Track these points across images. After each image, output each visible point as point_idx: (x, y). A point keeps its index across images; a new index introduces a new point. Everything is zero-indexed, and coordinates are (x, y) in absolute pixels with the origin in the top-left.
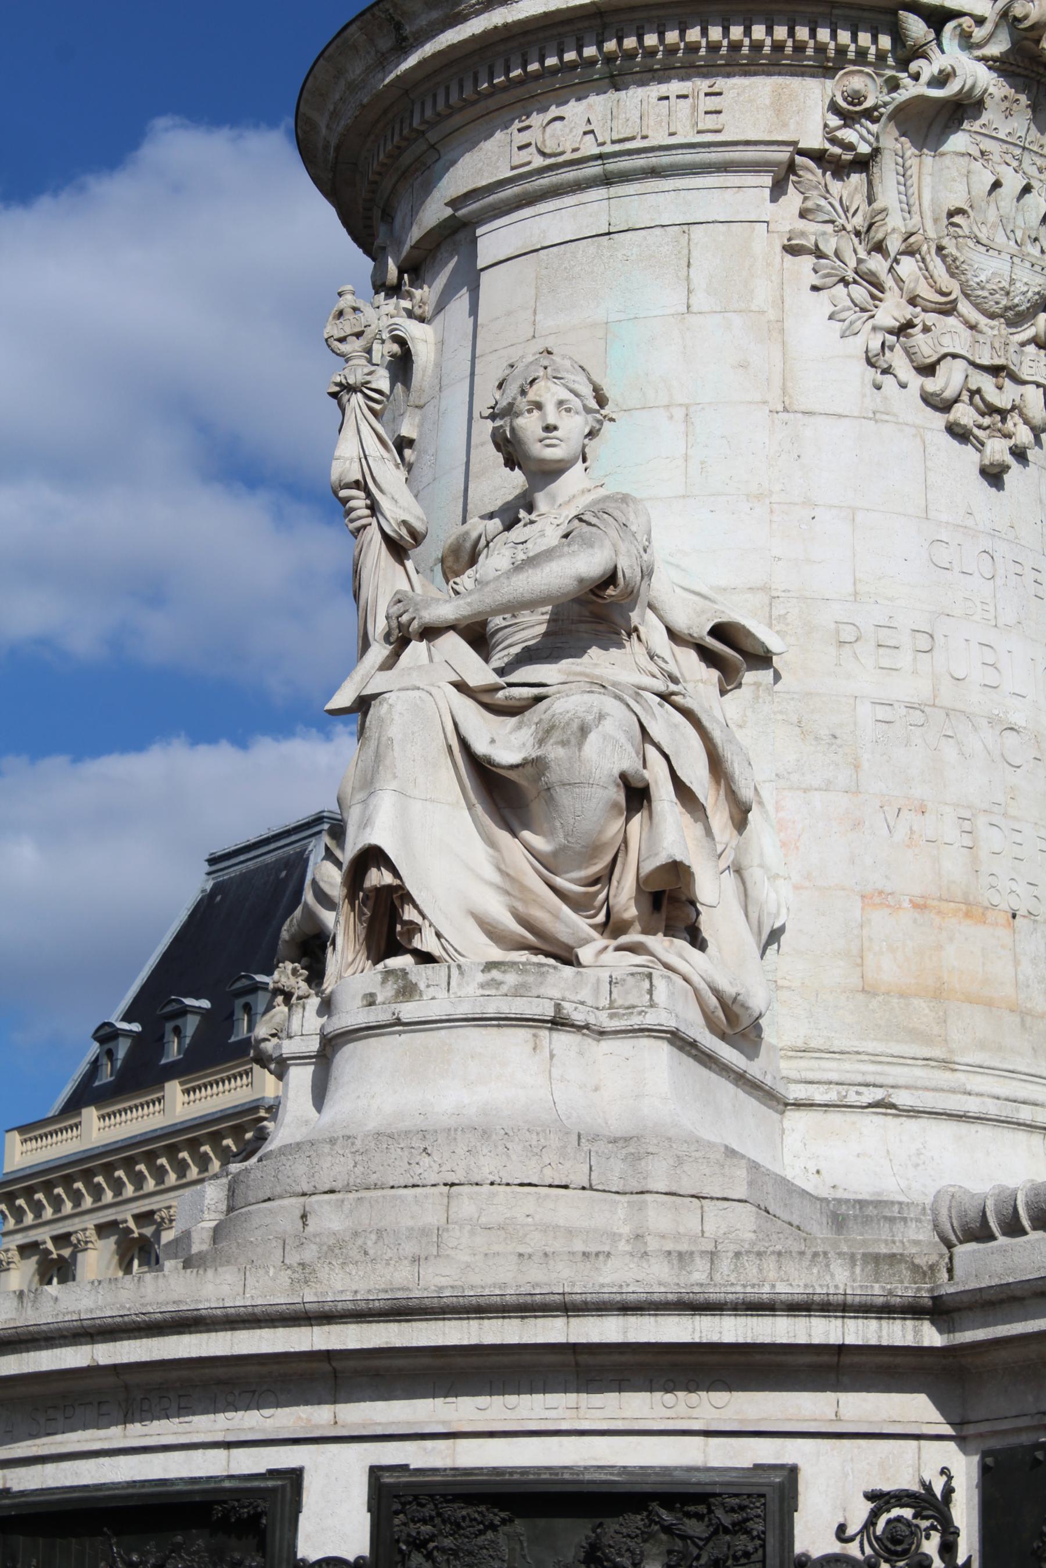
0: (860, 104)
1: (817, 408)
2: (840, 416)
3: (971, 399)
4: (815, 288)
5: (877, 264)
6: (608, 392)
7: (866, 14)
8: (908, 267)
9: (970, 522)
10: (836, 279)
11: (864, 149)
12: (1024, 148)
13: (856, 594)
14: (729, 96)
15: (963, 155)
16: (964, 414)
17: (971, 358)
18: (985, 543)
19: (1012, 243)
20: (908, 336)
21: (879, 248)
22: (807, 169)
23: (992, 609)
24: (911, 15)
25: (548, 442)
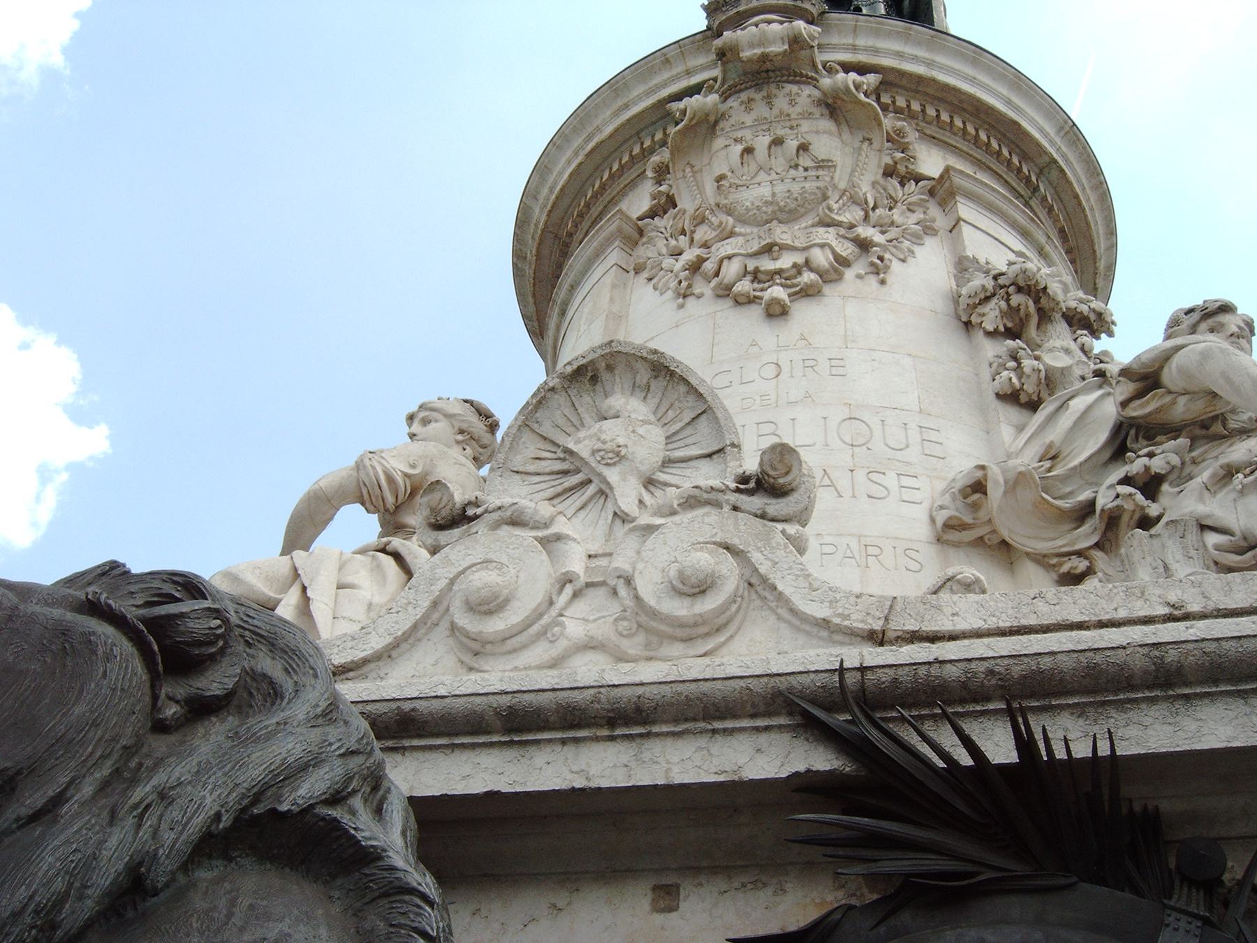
16: (745, 286)
21: (683, 233)
22: (647, 225)
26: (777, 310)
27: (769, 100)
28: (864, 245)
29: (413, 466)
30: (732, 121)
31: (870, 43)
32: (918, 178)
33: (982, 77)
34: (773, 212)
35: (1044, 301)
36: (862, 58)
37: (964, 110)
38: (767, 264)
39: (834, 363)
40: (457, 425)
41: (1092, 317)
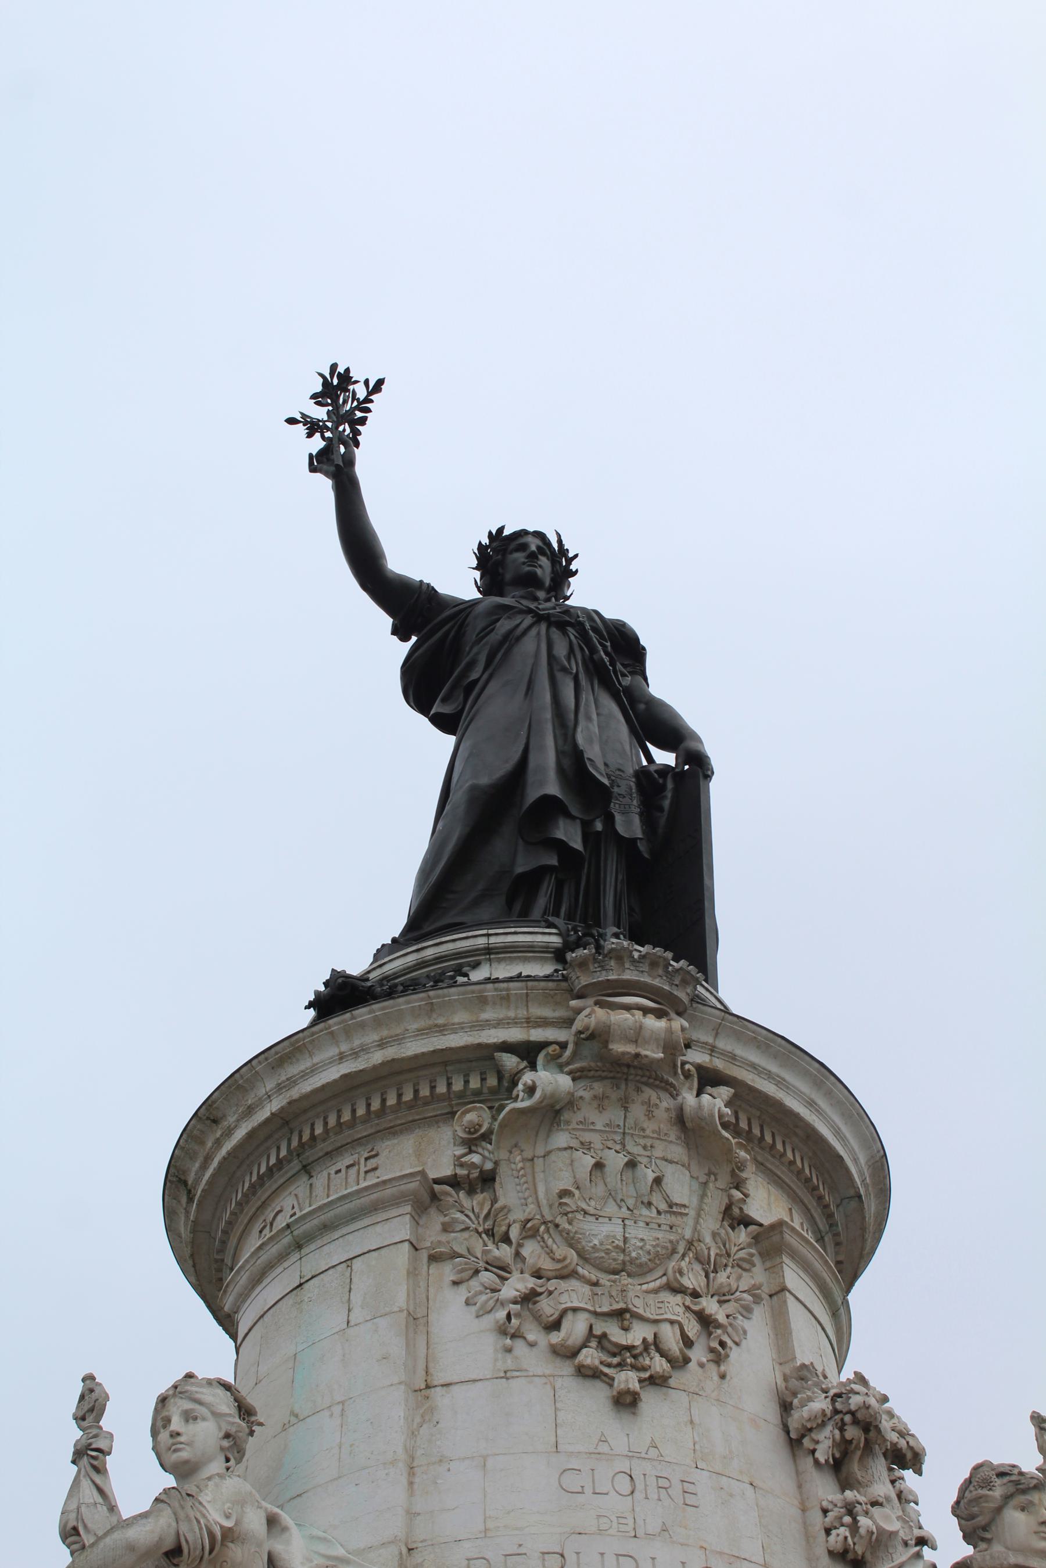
0: (476, 1131)
1: (456, 1379)
2: (475, 1381)
3: (599, 1343)
4: (456, 1283)
5: (504, 1252)
6: (252, 1400)
7: (474, 1064)
8: (530, 1250)
9: (604, 1448)
10: (471, 1272)
11: (489, 1166)
12: (624, 1133)
13: (486, 1530)
14: (384, 1154)
15: (565, 1149)
16: (590, 1356)
17: (592, 1309)
18: (624, 1465)
19: (624, 1209)
20: (535, 1303)
21: (506, 1239)
22: (447, 1194)
23: (631, 1521)
24: (504, 1054)
25: (174, 1447)
26: (629, 1399)
27: (625, 1104)
28: (706, 1321)
29: (228, 1517)
30: (579, 1116)
31: (729, 1048)
32: (747, 1222)
33: (822, 1103)
34: (624, 1263)
35: (872, 1434)
36: (719, 1064)
37: (796, 1134)
38: (617, 1336)
39: (690, 1488)
40: (225, 1427)
41: (909, 1455)
